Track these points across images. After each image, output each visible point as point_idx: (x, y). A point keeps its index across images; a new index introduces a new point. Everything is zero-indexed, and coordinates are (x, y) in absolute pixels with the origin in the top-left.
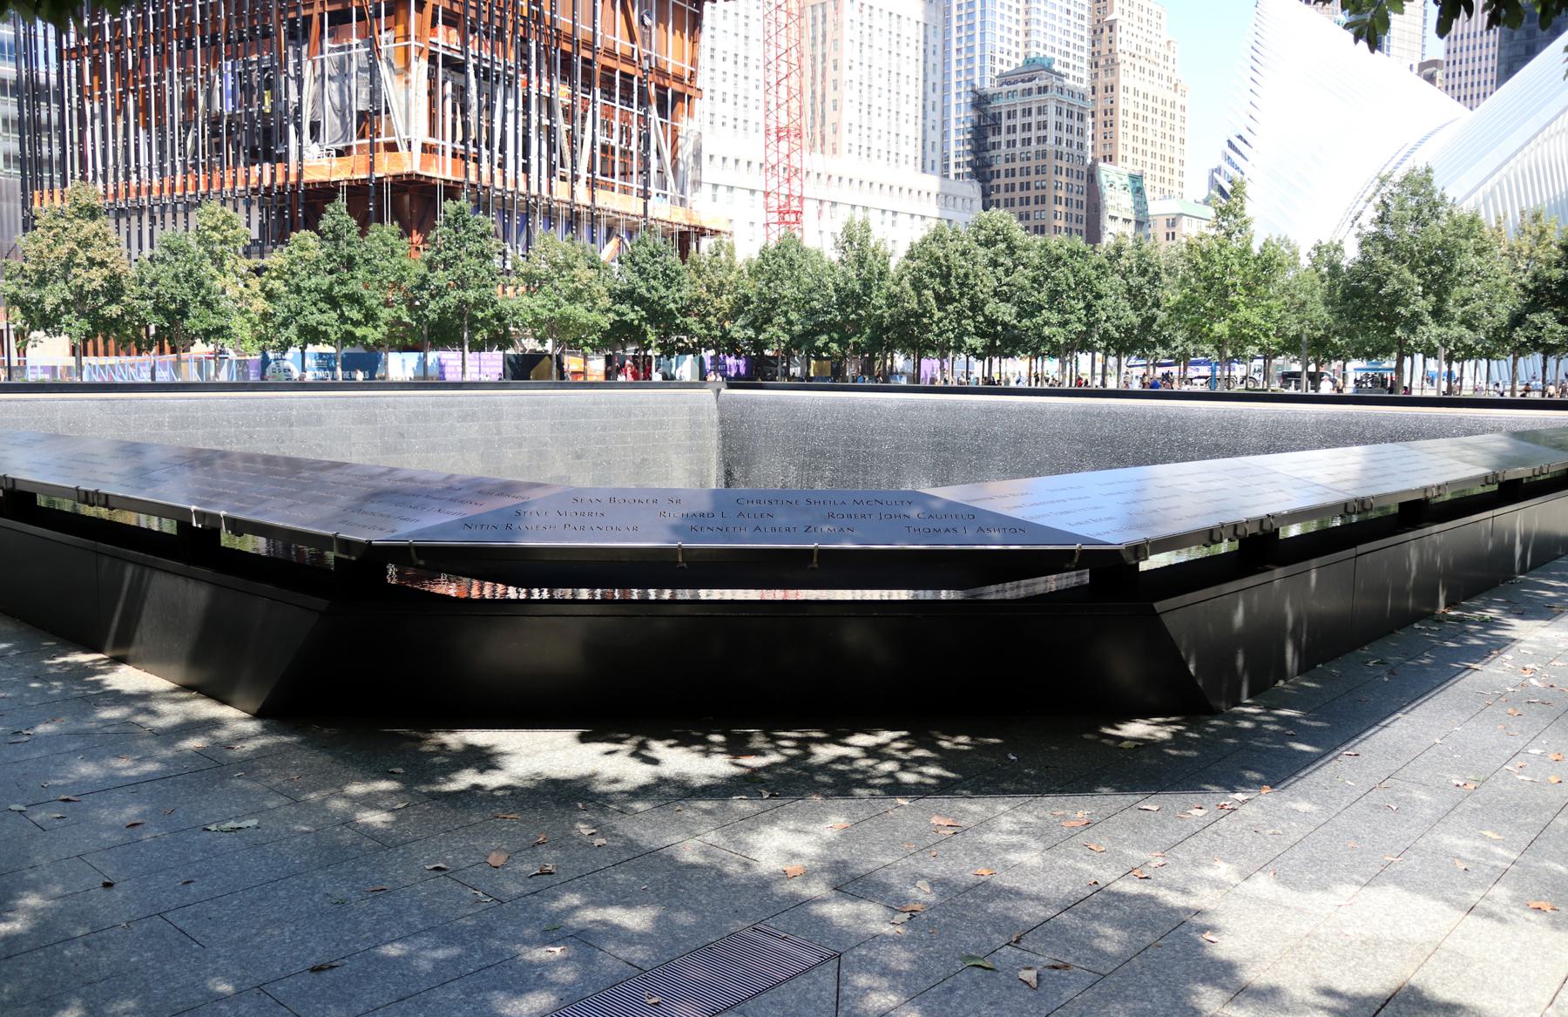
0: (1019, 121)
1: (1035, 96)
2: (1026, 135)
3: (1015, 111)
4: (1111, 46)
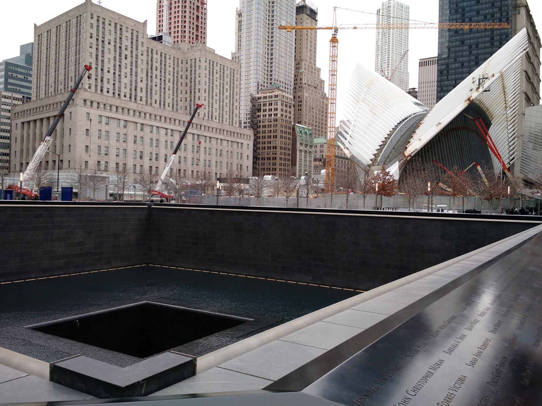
0: (267, 107)
1: (273, 99)
2: (270, 113)
3: (266, 104)
4: (301, 81)
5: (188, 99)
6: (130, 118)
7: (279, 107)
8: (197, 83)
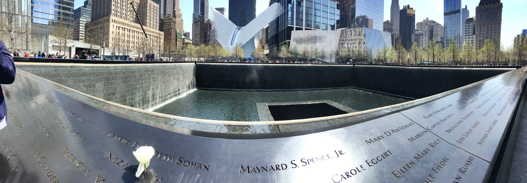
0: (167, 24)
8: (145, 13)
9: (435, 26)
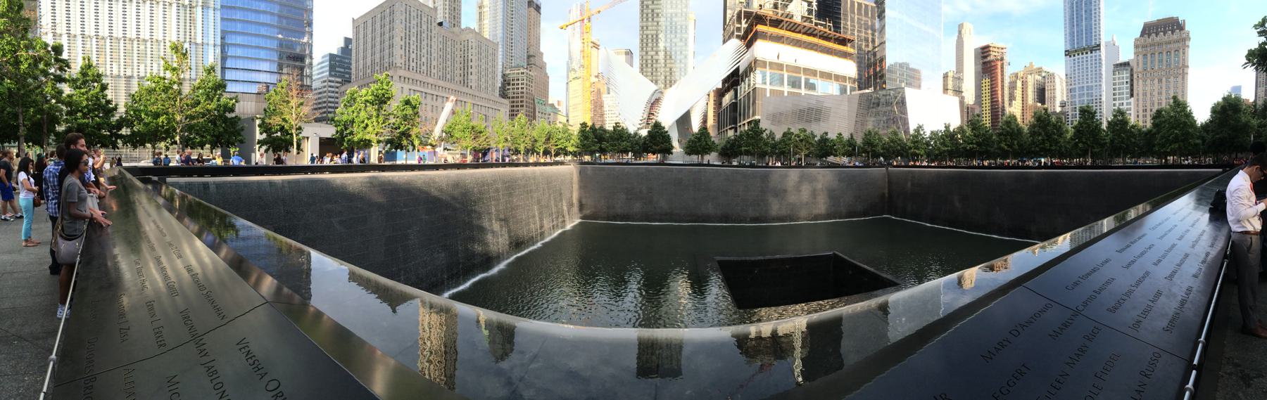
5: (462, 75)
6: (429, 91)
7: (525, 82)
9: (1049, 80)
